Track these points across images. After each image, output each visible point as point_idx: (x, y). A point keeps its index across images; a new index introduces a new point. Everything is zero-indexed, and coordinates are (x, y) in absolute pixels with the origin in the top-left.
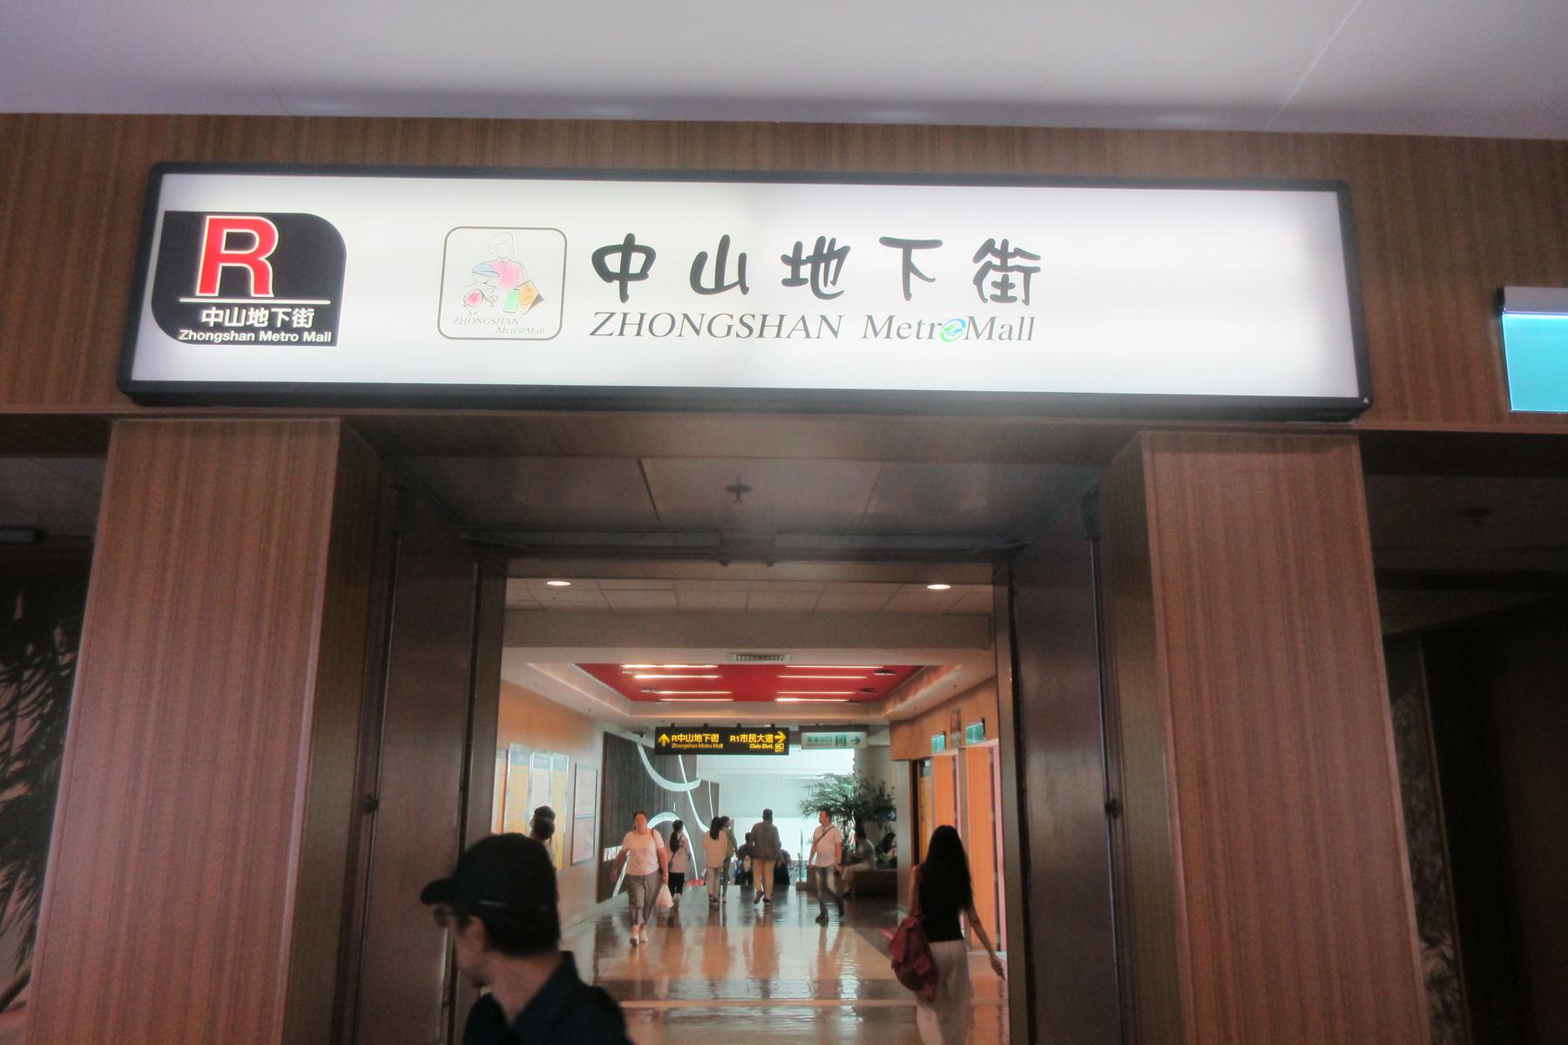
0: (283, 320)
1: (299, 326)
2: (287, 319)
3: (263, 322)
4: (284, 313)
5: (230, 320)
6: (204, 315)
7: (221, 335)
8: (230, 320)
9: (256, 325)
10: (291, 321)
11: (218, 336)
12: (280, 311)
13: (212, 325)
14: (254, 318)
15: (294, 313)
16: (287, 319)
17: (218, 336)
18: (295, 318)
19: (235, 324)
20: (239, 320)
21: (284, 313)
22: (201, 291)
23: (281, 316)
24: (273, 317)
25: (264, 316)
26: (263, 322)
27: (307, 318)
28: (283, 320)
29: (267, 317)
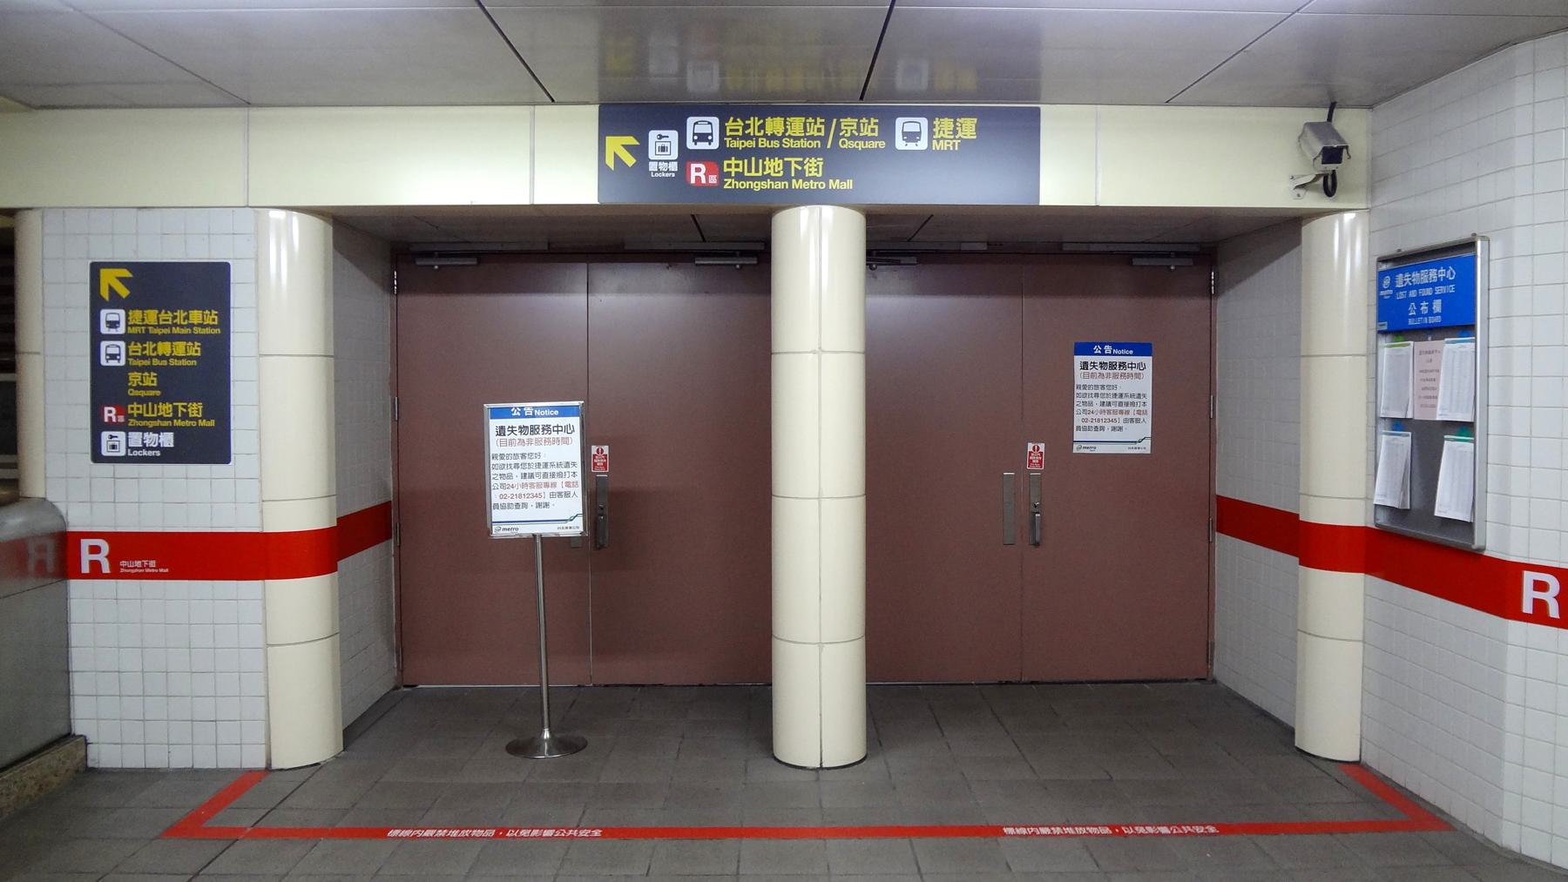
3: (779, 172)
7: (759, 183)
9: (773, 175)
11: (757, 185)
12: (793, 160)
14: (770, 168)
17: (757, 185)
19: (753, 174)
23: (793, 163)
24: (787, 165)
25: (779, 166)
26: (779, 172)
28: (795, 168)
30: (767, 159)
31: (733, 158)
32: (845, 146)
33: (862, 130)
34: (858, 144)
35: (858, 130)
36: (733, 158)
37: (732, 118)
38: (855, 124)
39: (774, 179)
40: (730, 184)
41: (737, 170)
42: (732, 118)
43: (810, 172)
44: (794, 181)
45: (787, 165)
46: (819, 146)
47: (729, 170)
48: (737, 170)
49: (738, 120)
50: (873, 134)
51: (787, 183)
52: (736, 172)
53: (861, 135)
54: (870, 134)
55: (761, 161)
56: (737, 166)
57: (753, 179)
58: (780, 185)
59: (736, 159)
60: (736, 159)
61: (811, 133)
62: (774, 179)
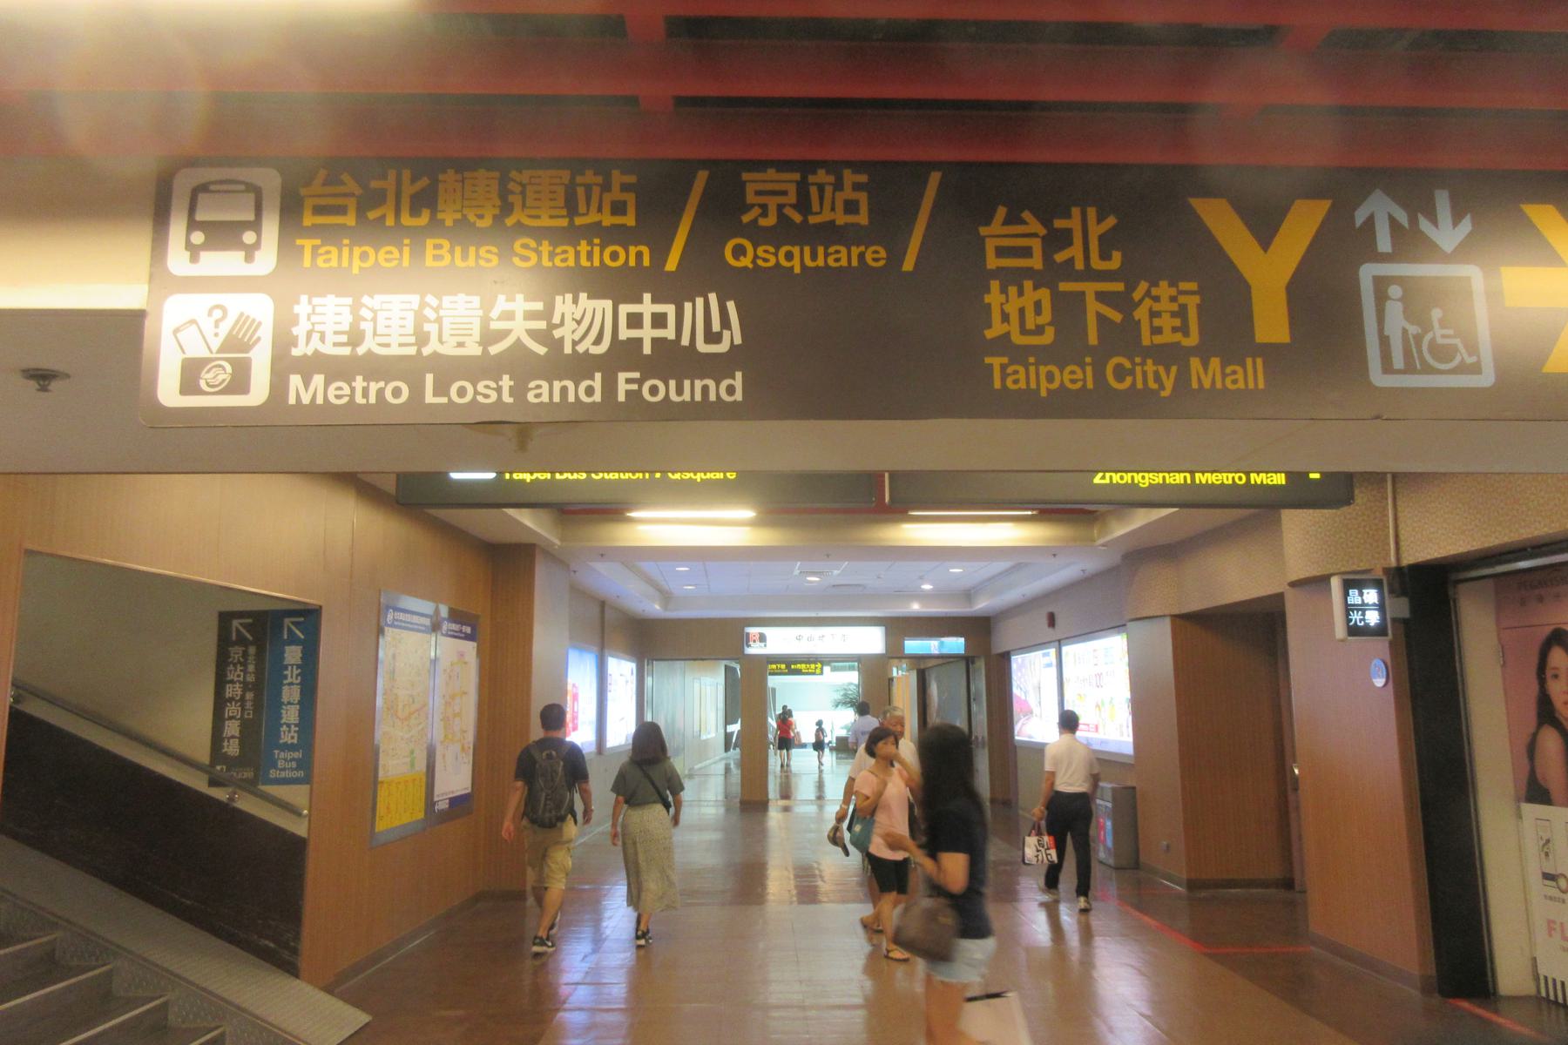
0: (1101, 318)
1: (1158, 339)
2: (1117, 317)
3: (1039, 330)
9: (1018, 339)
14: (1005, 318)
15: (1137, 295)
16: (1117, 317)
18: (1141, 314)
21: (1101, 297)
23: (1093, 307)
26: (1039, 330)
27: (1182, 313)
28: (1101, 318)
29: (1046, 316)
31: (647, 297)
32: (746, 262)
33: (815, 207)
34: (789, 256)
35: (803, 205)
36: (647, 297)
37: (1001, 212)
38: (792, 189)
41: (659, 333)
42: (1001, 212)
43: (1157, 331)
46: (646, 262)
47: (634, 333)
48: (659, 333)
49: (1026, 215)
50: (851, 219)
52: (655, 341)
53: (813, 220)
54: (841, 219)
59: (654, 301)
60: (654, 301)
61: (826, 216)
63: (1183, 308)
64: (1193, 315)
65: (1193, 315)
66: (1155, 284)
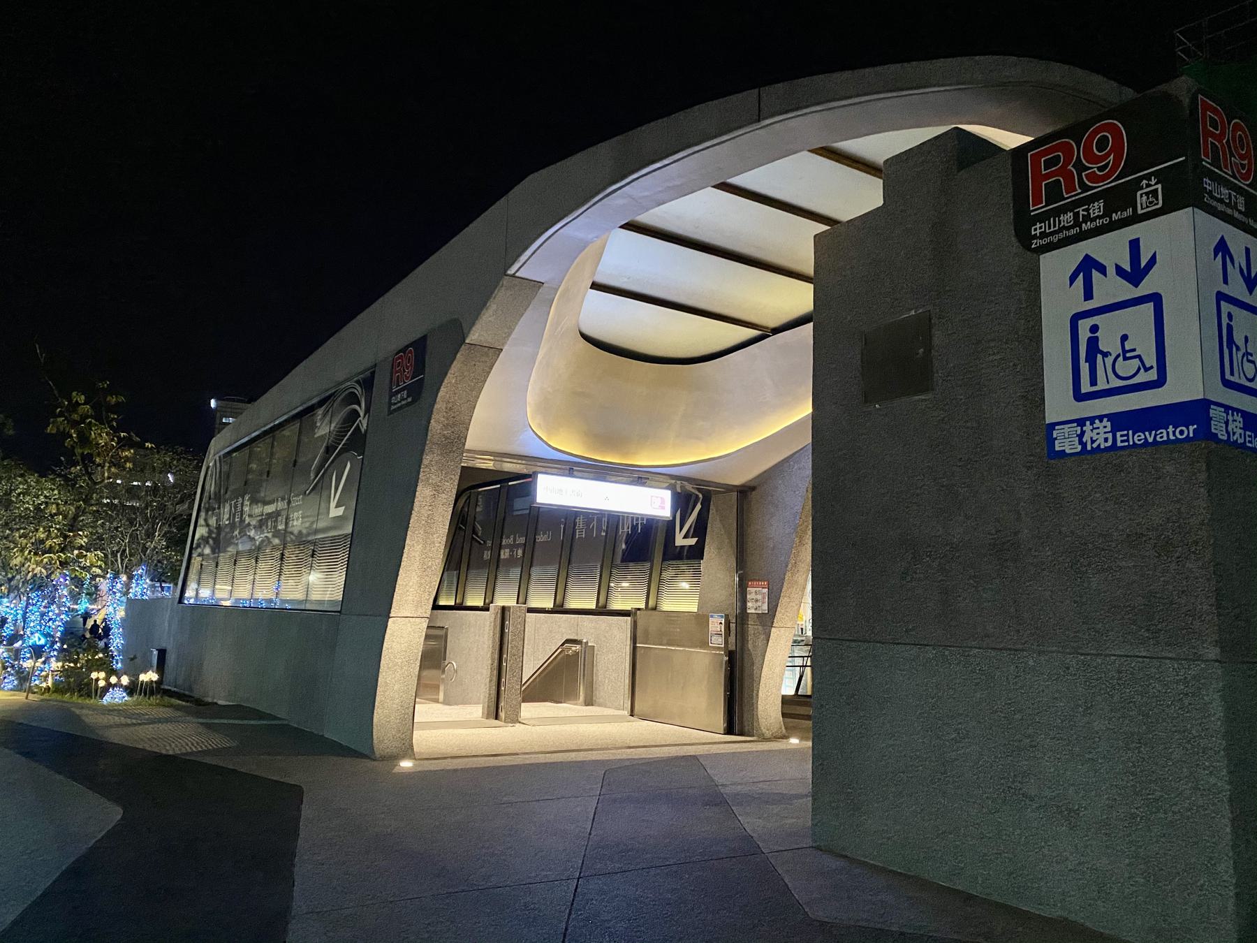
2: (1086, 213)
3: (1071, 221)
4: (1083, 210)
5: (1050, 228)
6: (1033, 230)
8: (1050, 228)
10: (1089, 214)
13: (1038, 235)
14: (1064, 221)
16: (1086, 213)
19: (1052, 230)
20: (1055, 226)
21: (1083, 210)
22: (1067, 194)
23: (1081, 213)
24: (1076, 215)
26: (1071, 221)
27: (1100, 208)
30: (1062, 215)
39: (1068, 228)
40: (1036, 244)
43: (1094, 214)
44: (1084, 225)
45: (1076, 215)
51: (1078, 228)
55: (1057, 219)
56: (1041, 228)
57: (1052, 234)
58: (1073, 232)
62: (1068, 228)
63: (1100, 207)
64: (1102, 208)
65: (1102, 208)
66: (1094, 203)
